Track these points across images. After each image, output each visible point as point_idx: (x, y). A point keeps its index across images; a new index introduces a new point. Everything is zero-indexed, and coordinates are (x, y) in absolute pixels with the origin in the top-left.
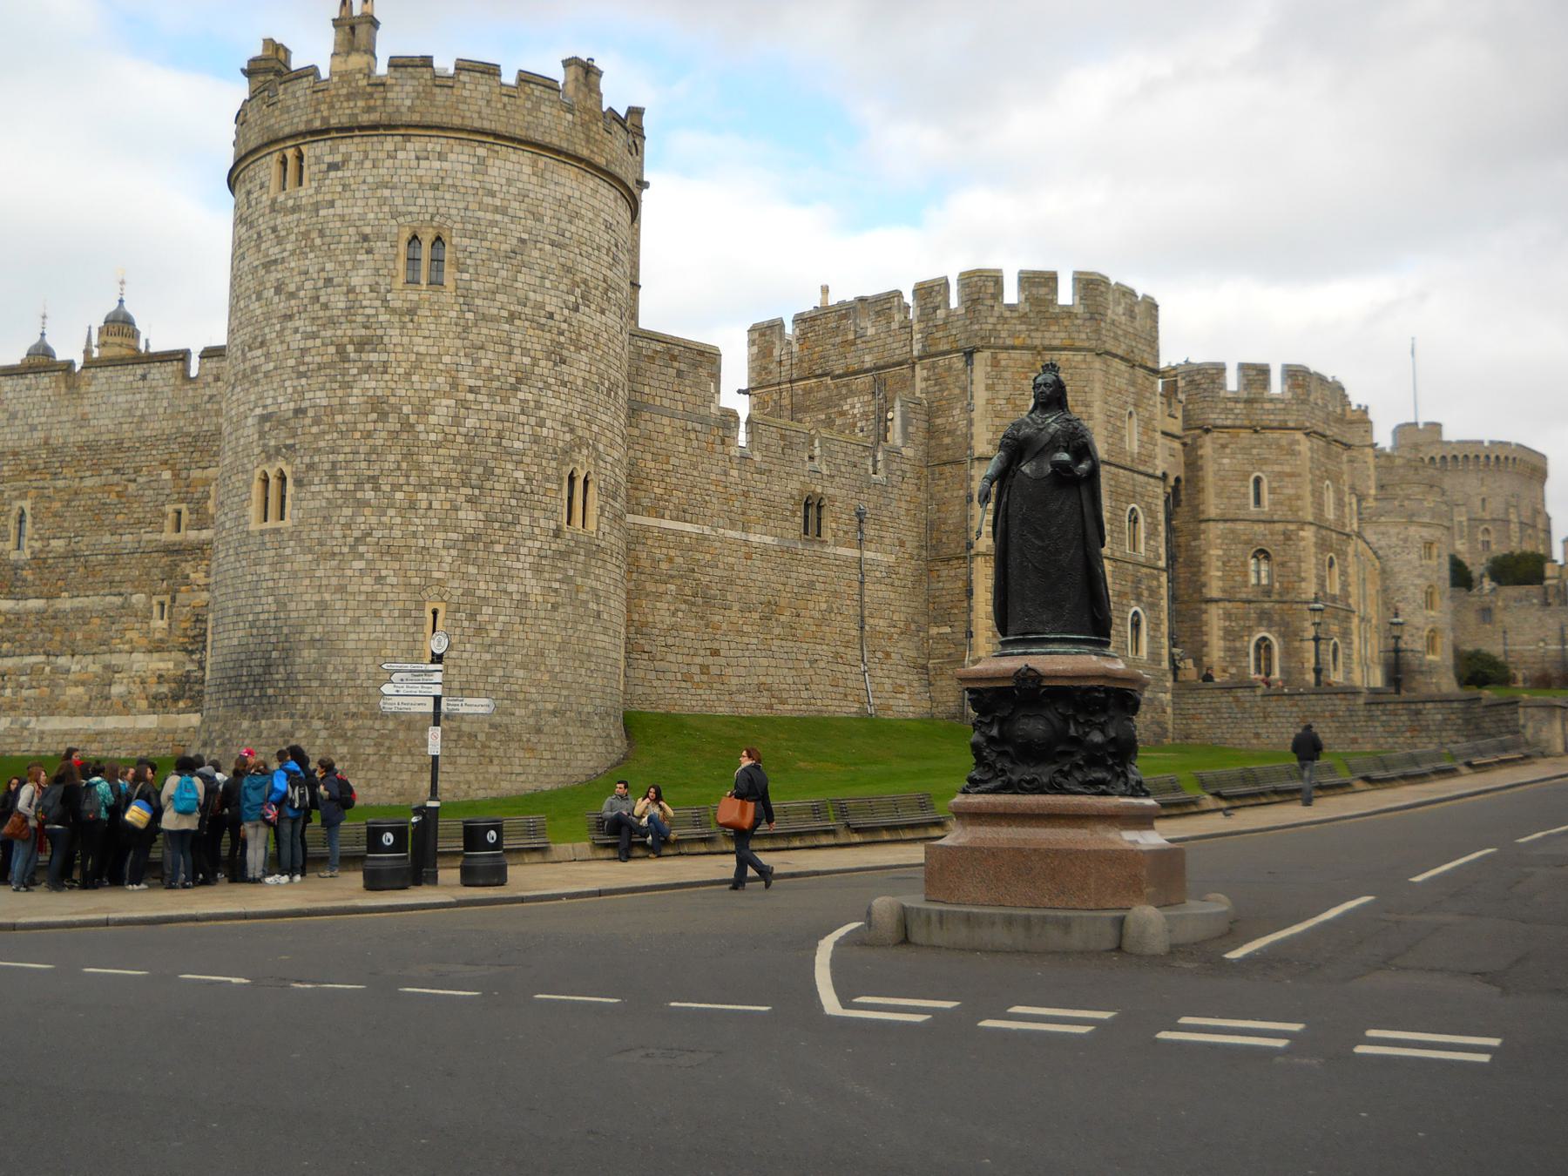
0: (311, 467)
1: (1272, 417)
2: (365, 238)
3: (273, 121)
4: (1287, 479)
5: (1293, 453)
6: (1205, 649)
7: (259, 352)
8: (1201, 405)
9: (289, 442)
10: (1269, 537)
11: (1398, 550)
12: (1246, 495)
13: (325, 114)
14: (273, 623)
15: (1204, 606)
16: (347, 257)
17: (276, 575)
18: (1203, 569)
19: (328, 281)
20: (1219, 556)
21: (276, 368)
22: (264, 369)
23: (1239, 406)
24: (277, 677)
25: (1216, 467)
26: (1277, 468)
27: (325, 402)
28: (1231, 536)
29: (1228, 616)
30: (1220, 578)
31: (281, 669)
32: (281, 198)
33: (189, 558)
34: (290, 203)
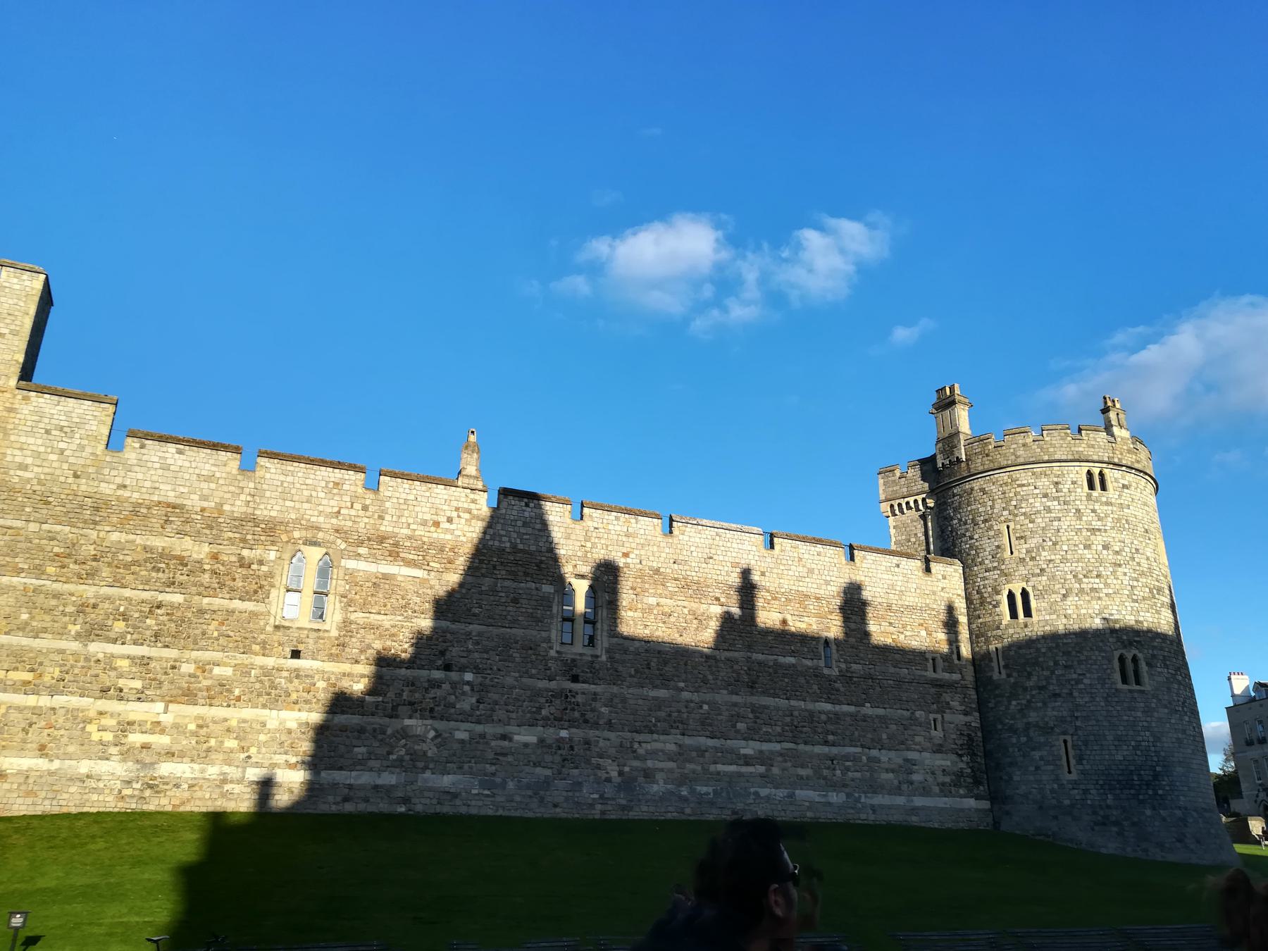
0: (1153, 656)
2: (1146, 531)
3: (1081, 449)
7: (1097, 580)
9: (1136, 639)
13: (1120, 456)
14: (1153, 749)
16: (1142, 540)
17: (1148, 719)
19: (1137, 550)
21: (1115, 593)
22: (1105, 591)
24: (1164, 783)
27: (1151, 620)
31: (1166, 778)
32: (1095, 494)
33: (948, 691)
34: (1104, 499)
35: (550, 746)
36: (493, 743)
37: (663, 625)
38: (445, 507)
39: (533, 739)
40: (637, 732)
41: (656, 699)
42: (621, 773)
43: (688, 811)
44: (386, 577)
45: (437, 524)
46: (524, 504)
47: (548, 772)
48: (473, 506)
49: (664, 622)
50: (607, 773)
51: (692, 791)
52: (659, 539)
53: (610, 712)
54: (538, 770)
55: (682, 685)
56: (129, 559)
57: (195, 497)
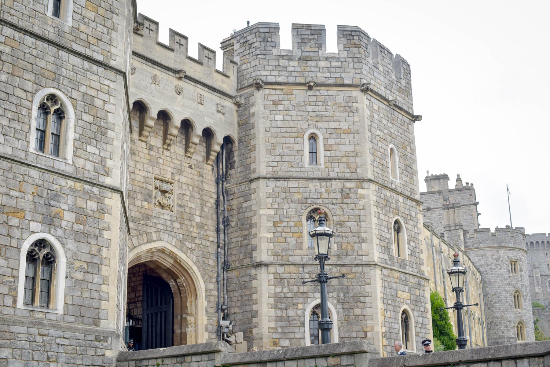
1: (327, 75)
4: (343, 136)
5: (350, 111)
6: (255, 320)
8: (253, 64)
10: (325, 195)
11: (494, 267)
12: (300, 153)
15: (253, 272)
18: (253, 231)
20: (268, 216)
23: (292, 63)
25: (268, 124)
26: (333, 125)
28: (283, 195)
29: (280, 281)
30: (271, 240)
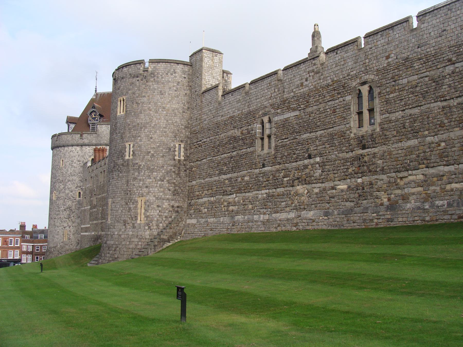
35: (352, 189)
36: (329, 192)
37: (412, 95)
38: (305, 74)
39: (345, 187)
40: (398, 171)
41: (409, 147)
42: (389, 200)
43: (427, 218)
44: (287, 120)
45: (302, 84)
46: (335, 53)
47: (352, 204)
48: (314, 67)
49: (413, 93)
50: (382, 200)
51: (432, 206)
52: (409, 35)
53: (383, 163)
54: (348, 204)
55: (426, 133)
56: (225, 142)
57: (236, 111)
